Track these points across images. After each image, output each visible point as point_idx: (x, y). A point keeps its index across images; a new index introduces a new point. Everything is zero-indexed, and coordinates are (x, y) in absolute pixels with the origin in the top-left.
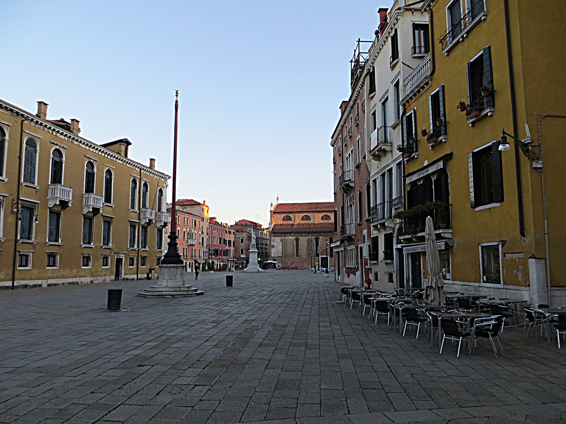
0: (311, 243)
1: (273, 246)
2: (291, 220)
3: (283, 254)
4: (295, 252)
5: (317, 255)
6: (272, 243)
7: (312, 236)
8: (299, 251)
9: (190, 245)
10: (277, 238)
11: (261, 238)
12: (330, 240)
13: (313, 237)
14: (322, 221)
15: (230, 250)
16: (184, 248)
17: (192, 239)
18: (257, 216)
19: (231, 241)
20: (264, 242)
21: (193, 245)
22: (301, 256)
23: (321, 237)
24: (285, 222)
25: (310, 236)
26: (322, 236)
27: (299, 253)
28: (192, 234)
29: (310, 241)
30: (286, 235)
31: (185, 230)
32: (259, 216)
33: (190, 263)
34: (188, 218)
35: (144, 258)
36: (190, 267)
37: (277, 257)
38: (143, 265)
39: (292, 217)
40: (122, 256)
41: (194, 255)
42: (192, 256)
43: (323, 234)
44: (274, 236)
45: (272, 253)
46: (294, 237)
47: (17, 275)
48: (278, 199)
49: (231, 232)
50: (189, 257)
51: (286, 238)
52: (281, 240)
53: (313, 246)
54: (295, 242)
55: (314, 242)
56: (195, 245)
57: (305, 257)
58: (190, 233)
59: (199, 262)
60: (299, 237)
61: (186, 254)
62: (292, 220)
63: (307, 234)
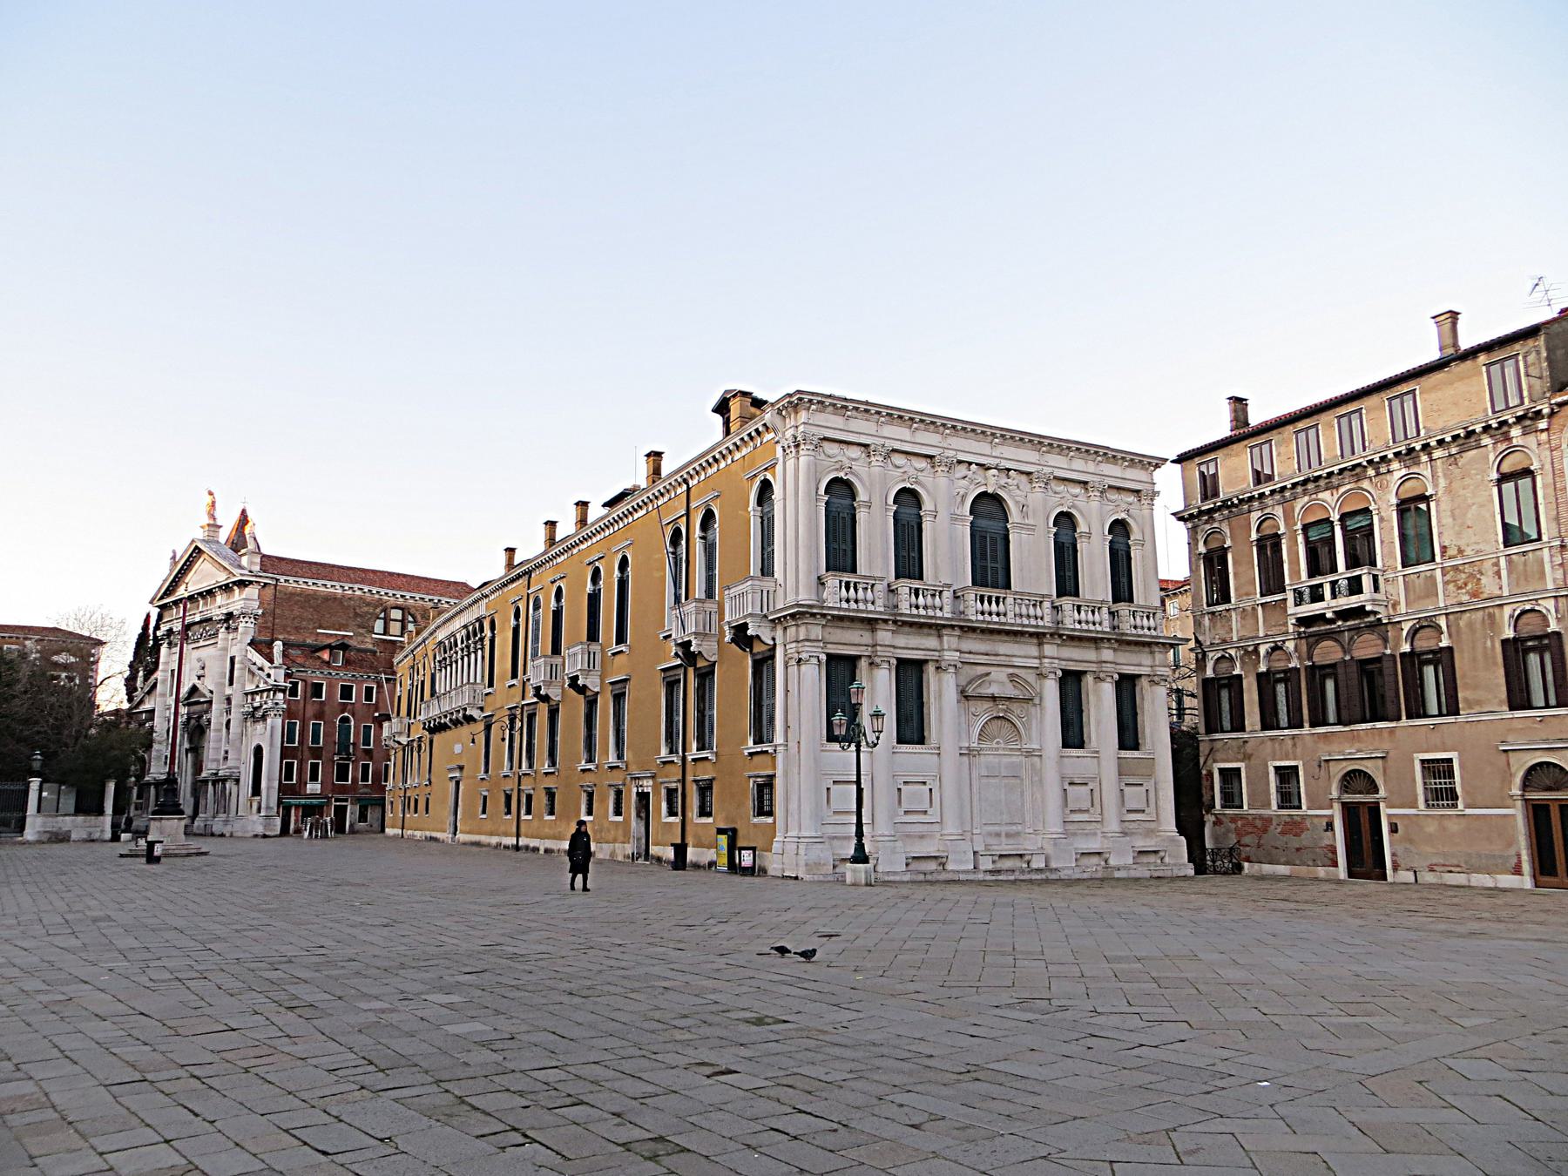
35: (705, 789)
38: (704, 812)
40: (647, 785)
47: (523, 829)
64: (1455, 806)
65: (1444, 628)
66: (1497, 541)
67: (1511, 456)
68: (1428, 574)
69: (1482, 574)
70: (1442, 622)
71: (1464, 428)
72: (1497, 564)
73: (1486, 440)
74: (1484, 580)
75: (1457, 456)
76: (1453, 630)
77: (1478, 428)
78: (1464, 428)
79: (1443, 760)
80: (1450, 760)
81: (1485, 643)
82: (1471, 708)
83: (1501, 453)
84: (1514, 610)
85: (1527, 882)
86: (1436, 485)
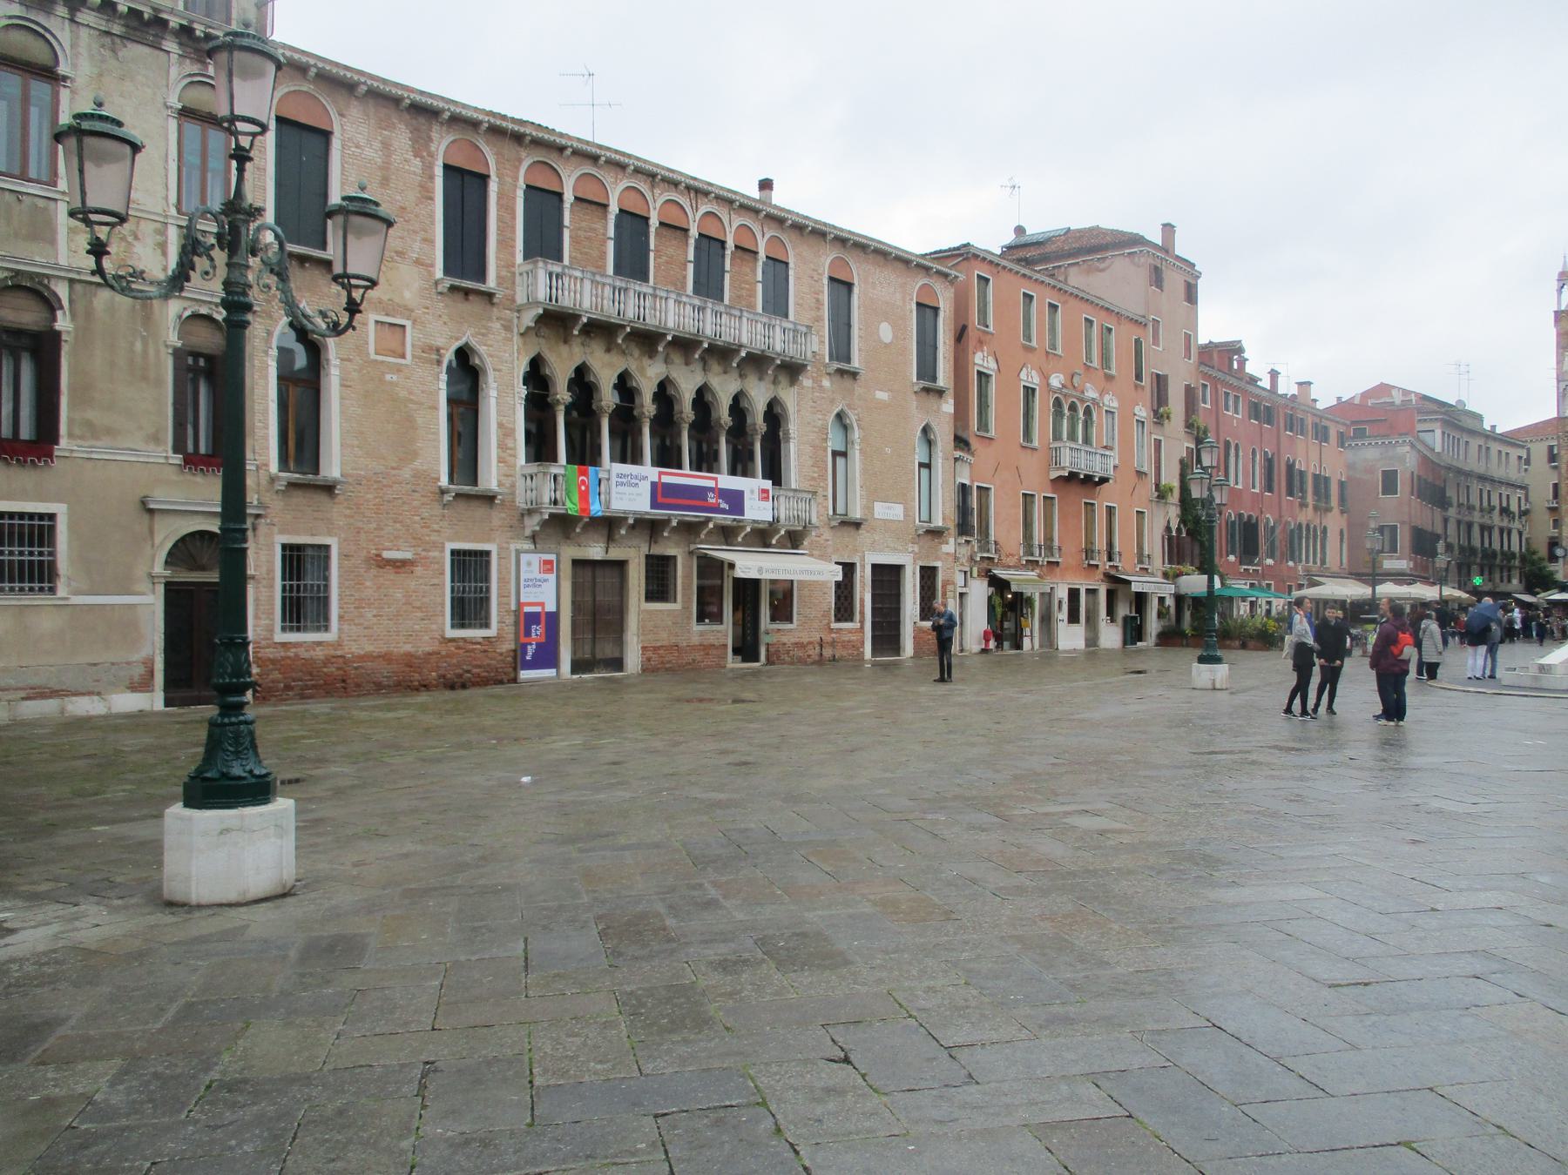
9: (1073, 476)
11: (1482, 478)
15: (1324, 531)
16: (1028, 498)
17: (1087, 441)
19: (1327, 480)
20: (1495, 502)
21: (1088, 478)
28: (1088, 412)
31: (1031, 377)
32: (1463, 369)
33: (1074, 594)
34: (1053, 307)
36: (1073, 618)
41: (1100, 543)
42: (1089, 552)
49: (1326, 428)
50: (1069, 553)
56: (1104, 480)
58: (1073, 408)
59: (1135, 588)
61: (1049, 538)
64: (52, 590)
65: (65, 303)
66: (166, 198)
67: (200, 88)
68: (41, 203)
69: (136, 238)
70: (62, 291)
71: (155, 9)
72: (162, 232)
73: (171, 45)
74: (138, 248)
75: (118, 41)
76: (80, 306)
77: (174, 22)
78: (155, 9)
79: (41, 516)
80: (52, 517)
81: (132, 344)
82: (97, 438)
83: (190, 75)
84: (185, 309)
85: (154, 700)
86: (74, 66)
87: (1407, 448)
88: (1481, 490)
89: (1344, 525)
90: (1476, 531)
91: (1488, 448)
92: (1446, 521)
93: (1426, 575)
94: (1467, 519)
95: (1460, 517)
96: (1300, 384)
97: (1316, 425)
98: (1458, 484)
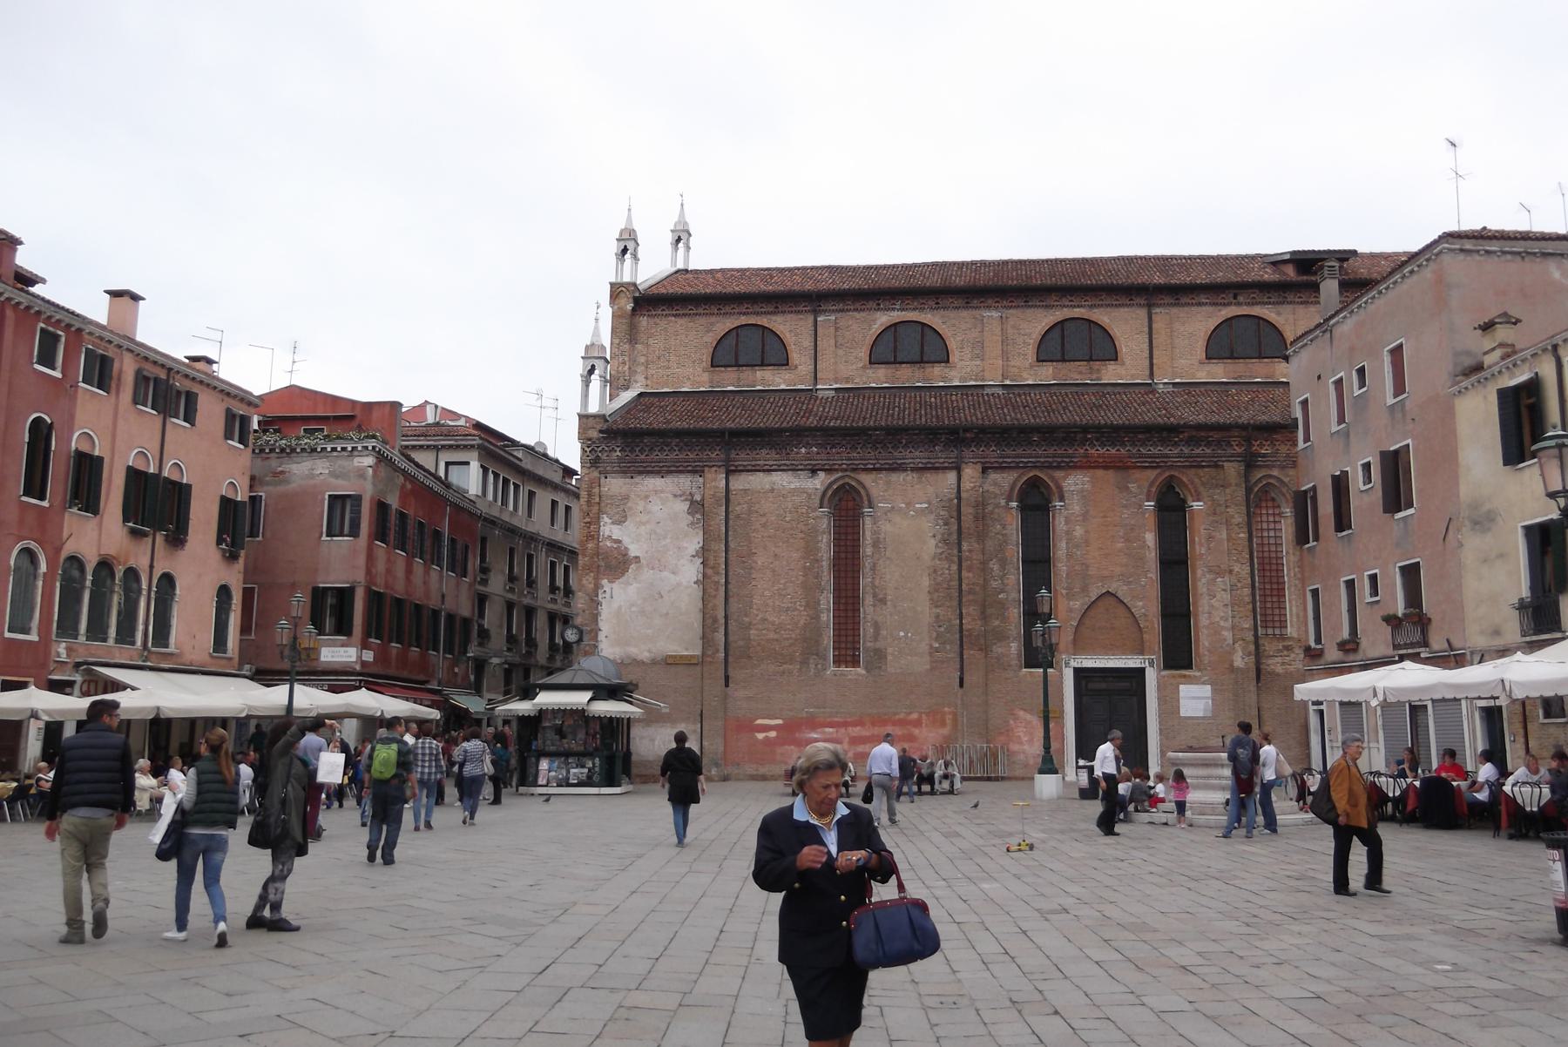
0: (981, 536)
1: (618, 564)
2: (784, 362)
3: (706, 639)
4: (827, 617)
5: (1039, 656)
6: (609, 529)
7: (984, 470)
8: (868, 609)
10: (653, 483)
12: (1161, 508)
13: (1003, 481)
14: (1047, 374)
18: (540, 395)
22: (880, 655)
23: (1074, 482)
24: (730, 381)
25: (970, 472)
26: (1088, 465)
27: (866, 630)
29: (967, 511)
30: (742, 457)
37: (654, 662)
39: (789, 339)
43: (1096, 451)
44: (632, 470)
45: (605, 625)
46: (819, 482)
48: (680, 237)
51: (740, 482)
52: (697, 507)
53: (995, 566)
54: (823, 521)
55: (1011, 525)
57: (920, 664)
60: (867, 479)
62: (795, 357)
63: (941, 455)
87: (369, 461)
88: (553, 564)
89: (234, 578)
90: (541, 621)
91: (568, 509)
92: (482, 600)
93: (422, 677)
94: (527, 601)
95: (510, 596)
96: (115, 294)
97: (141, 379)
98: (512, 551)
